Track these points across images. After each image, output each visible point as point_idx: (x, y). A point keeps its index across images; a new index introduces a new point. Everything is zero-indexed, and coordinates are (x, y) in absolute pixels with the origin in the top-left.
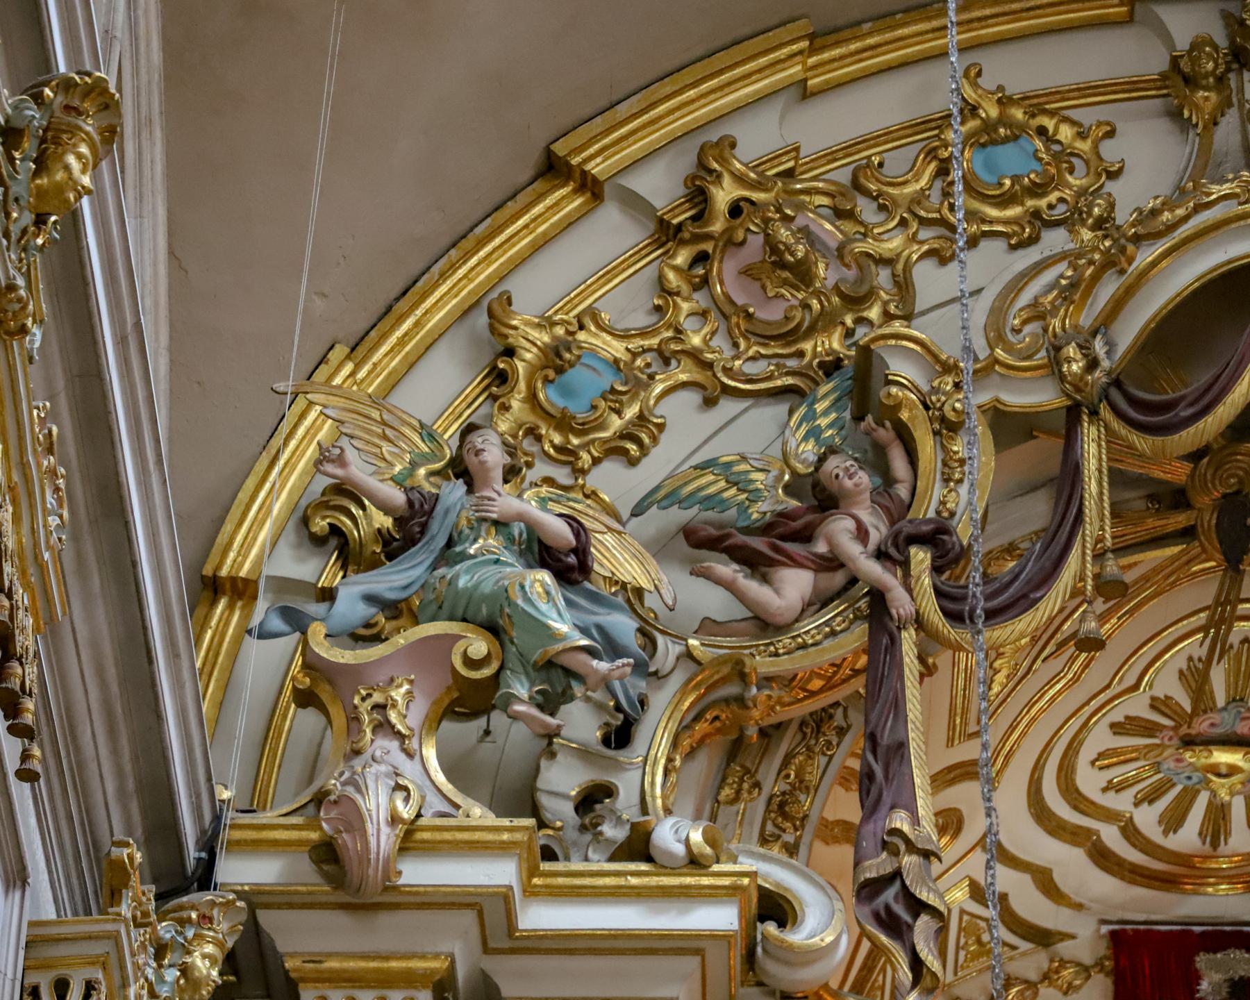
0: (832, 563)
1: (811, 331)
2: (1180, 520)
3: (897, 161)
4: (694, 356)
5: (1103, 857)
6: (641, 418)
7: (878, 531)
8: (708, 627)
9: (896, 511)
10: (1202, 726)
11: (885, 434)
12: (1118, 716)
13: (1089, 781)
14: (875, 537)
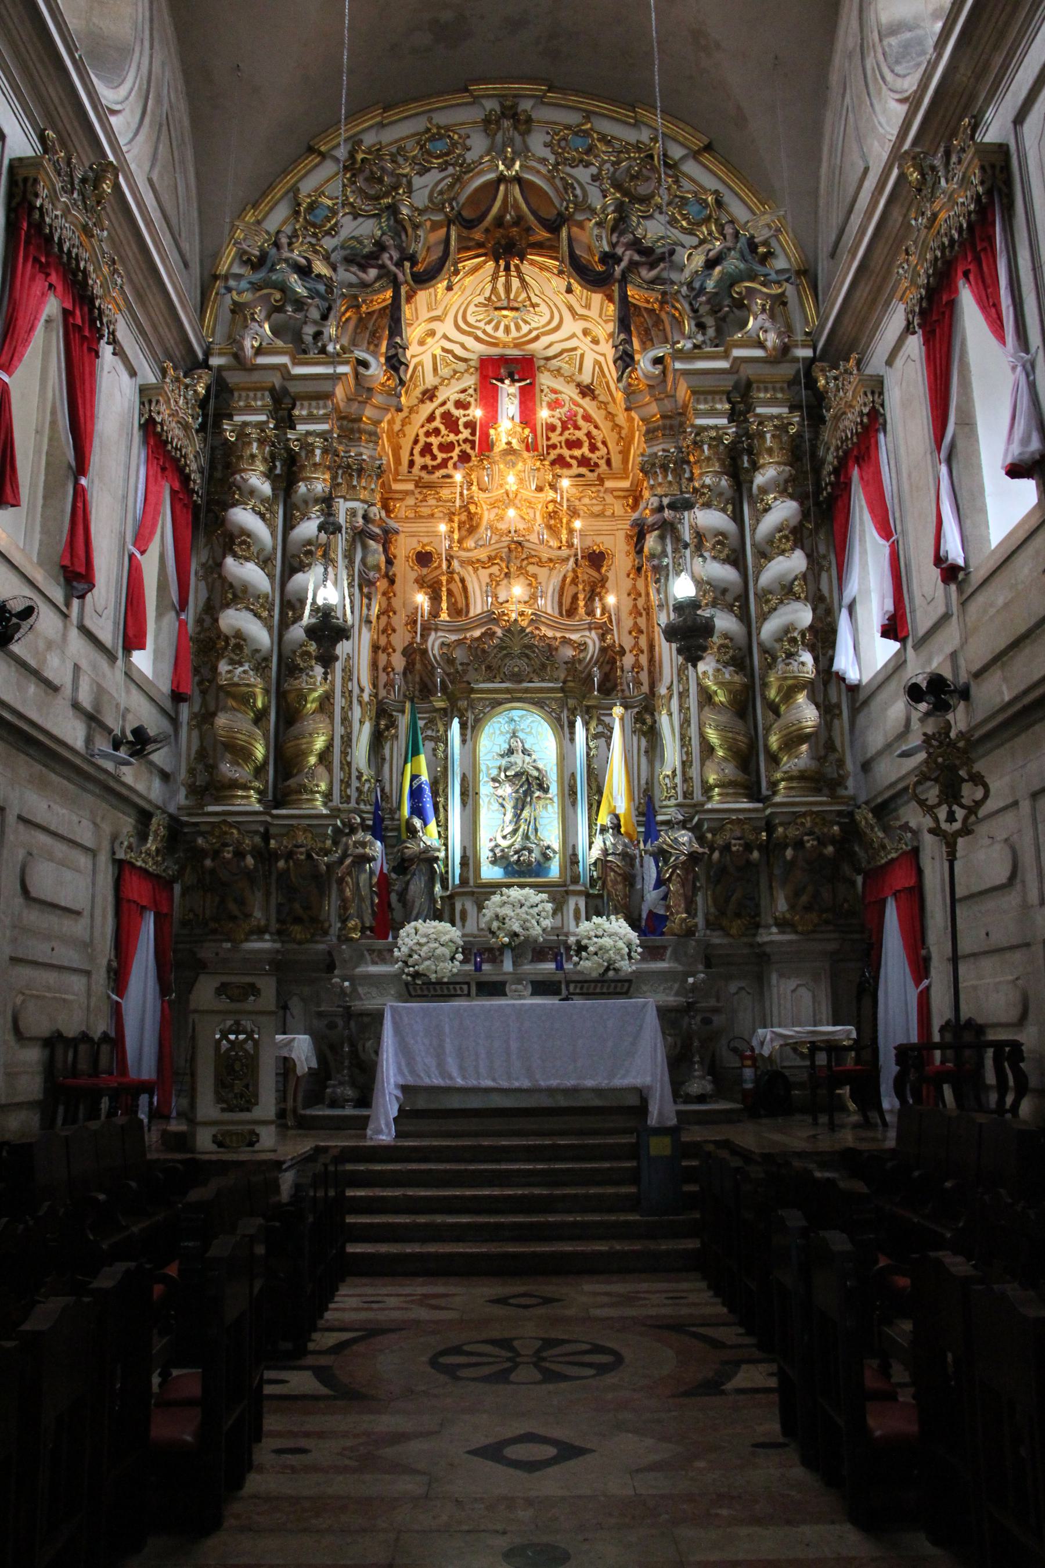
1: (383, 198)
2: (481, 251)
3: (410, 144)
4: (351, 204)
5: (477, 339)
6: (336, 224)
7: (396, 256)
8: (351, 285)
9: (401, 249)
10: (499, 305)
11: (399, 228)
13: (471, 319)
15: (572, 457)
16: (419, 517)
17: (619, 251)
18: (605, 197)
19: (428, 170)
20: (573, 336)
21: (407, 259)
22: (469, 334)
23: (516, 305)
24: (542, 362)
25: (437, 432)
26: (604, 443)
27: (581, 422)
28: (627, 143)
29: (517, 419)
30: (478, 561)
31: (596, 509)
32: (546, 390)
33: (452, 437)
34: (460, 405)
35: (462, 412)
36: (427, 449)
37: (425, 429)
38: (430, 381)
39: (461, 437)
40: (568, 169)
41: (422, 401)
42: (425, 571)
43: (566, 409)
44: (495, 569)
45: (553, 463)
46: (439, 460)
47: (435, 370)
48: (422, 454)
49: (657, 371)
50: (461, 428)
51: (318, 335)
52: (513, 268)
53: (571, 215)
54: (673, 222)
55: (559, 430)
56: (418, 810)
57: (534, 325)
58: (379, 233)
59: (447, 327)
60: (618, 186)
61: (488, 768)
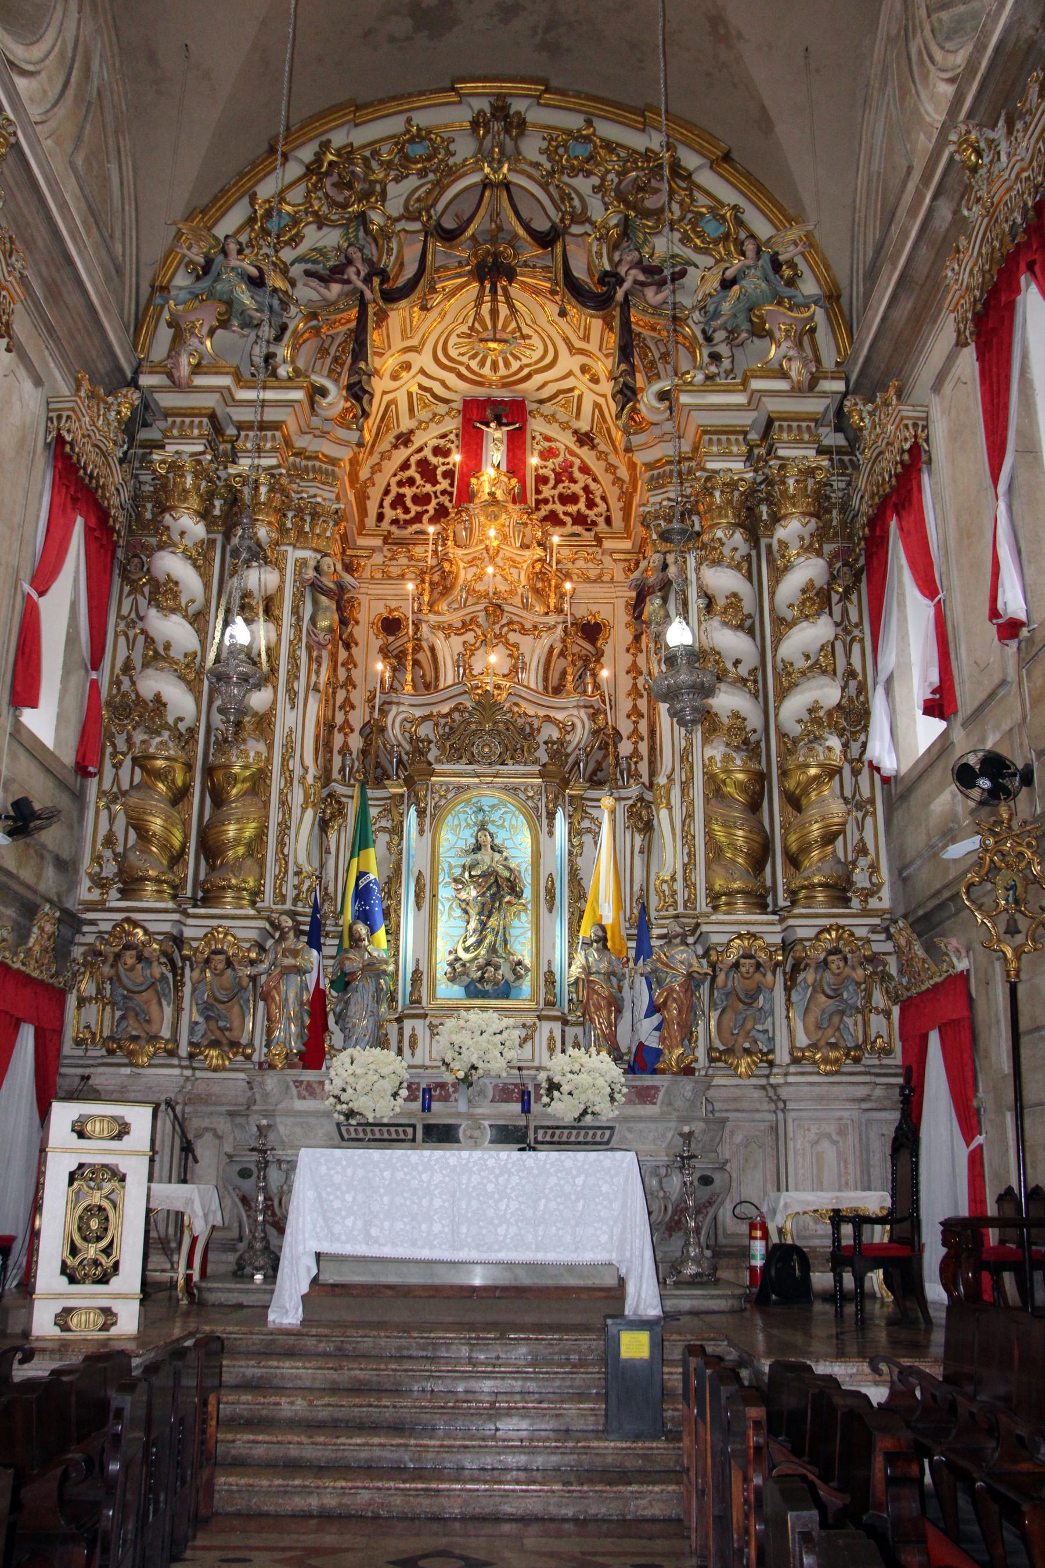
0: (348, 282)
5: (460, 376)
6: (297, 234)
10: (484, 335)
12: (458, 332)
13: (453, 353)
14: (363, 274)
15: (565, 514)
16: (387, 576)
17: (622, 270)
18: (607, 209)
19: (407, 176)
20: (570, 374)
21: (376, 274)
22: (450, 370)
23: (505, 336)
24: (535, 406)
25: (411, 482)
26: (604, 499)
27: (577, 474)
28: (635, 152)
29: (504, 468)
30: (450, 626)
31: (593, 574)
32: (539, 437)
33: (428, 488)
34: (437, 451)
35: (441, 460)
36: (399, 501)
37: (398, 478)
38: (406, 424)
39: (439, 488)
40: (565, 178)
41: (395, 447)
42: (391, 639)
43: (560, 459)
44: (469, 637)
45: (545, 519)
46: (412, 514)
47: (411, 410)
48: (393, 506)
49: (663, 406)
50: (439, 478)
51: (269, 357)
52: (500, 291)
53: (566, 228)
54: (685, 240)
55: (552, 482)
56: (364, 916)
57: (525, 361)
58: (346, 245)
59: (424, 360)
60: (621, 197)
61: (450, 866)
